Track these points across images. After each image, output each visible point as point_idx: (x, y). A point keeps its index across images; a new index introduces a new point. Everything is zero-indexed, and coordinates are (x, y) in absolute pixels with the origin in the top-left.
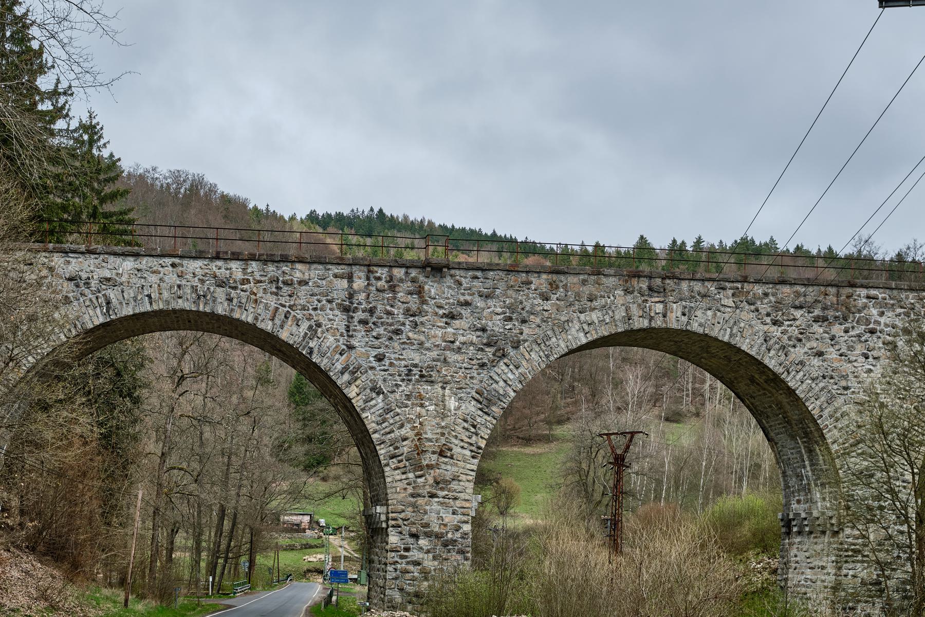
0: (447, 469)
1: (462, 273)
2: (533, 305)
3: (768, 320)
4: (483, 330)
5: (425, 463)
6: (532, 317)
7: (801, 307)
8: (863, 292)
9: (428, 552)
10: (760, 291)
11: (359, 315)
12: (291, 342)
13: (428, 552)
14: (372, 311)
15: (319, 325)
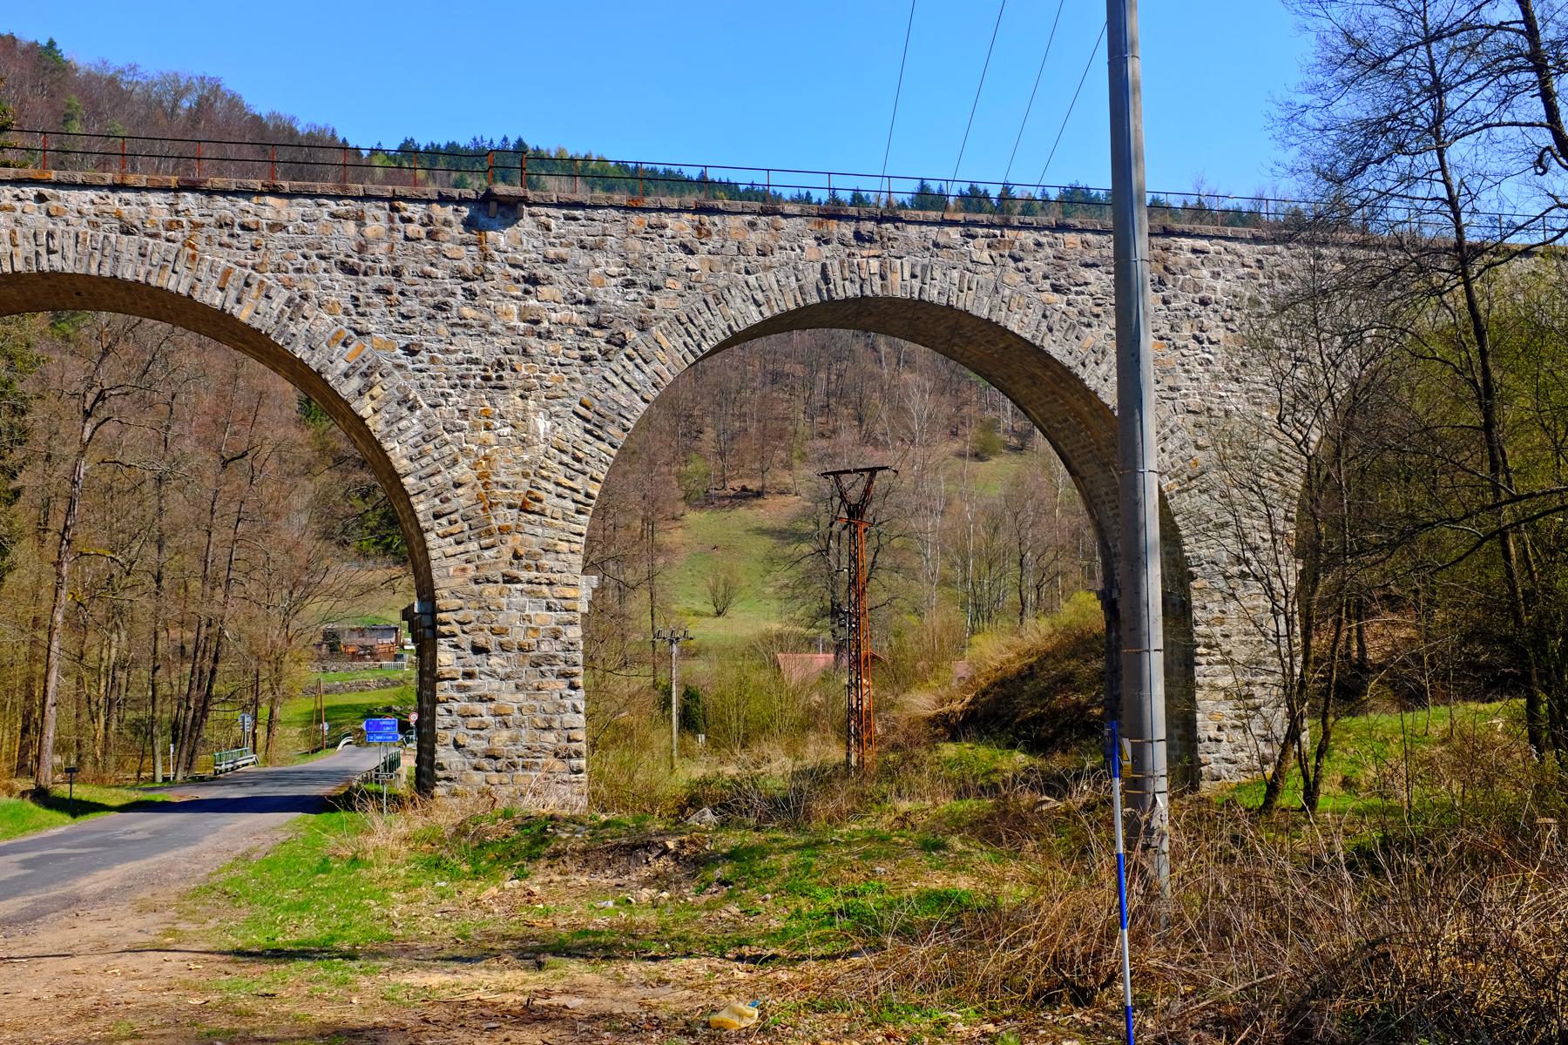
1: (552, 211)
2: (669, 263)
3: (1046, 285)
4: (589, 302)
5: (495, 524)
6: (670, 280)
7: (1094, 265)
8: (1187, 243)
9: (508, 677)
10: (1030, 242)
12: (256, 325)
13: (508, 677)
14: (397, 273)
15: (305, 297)
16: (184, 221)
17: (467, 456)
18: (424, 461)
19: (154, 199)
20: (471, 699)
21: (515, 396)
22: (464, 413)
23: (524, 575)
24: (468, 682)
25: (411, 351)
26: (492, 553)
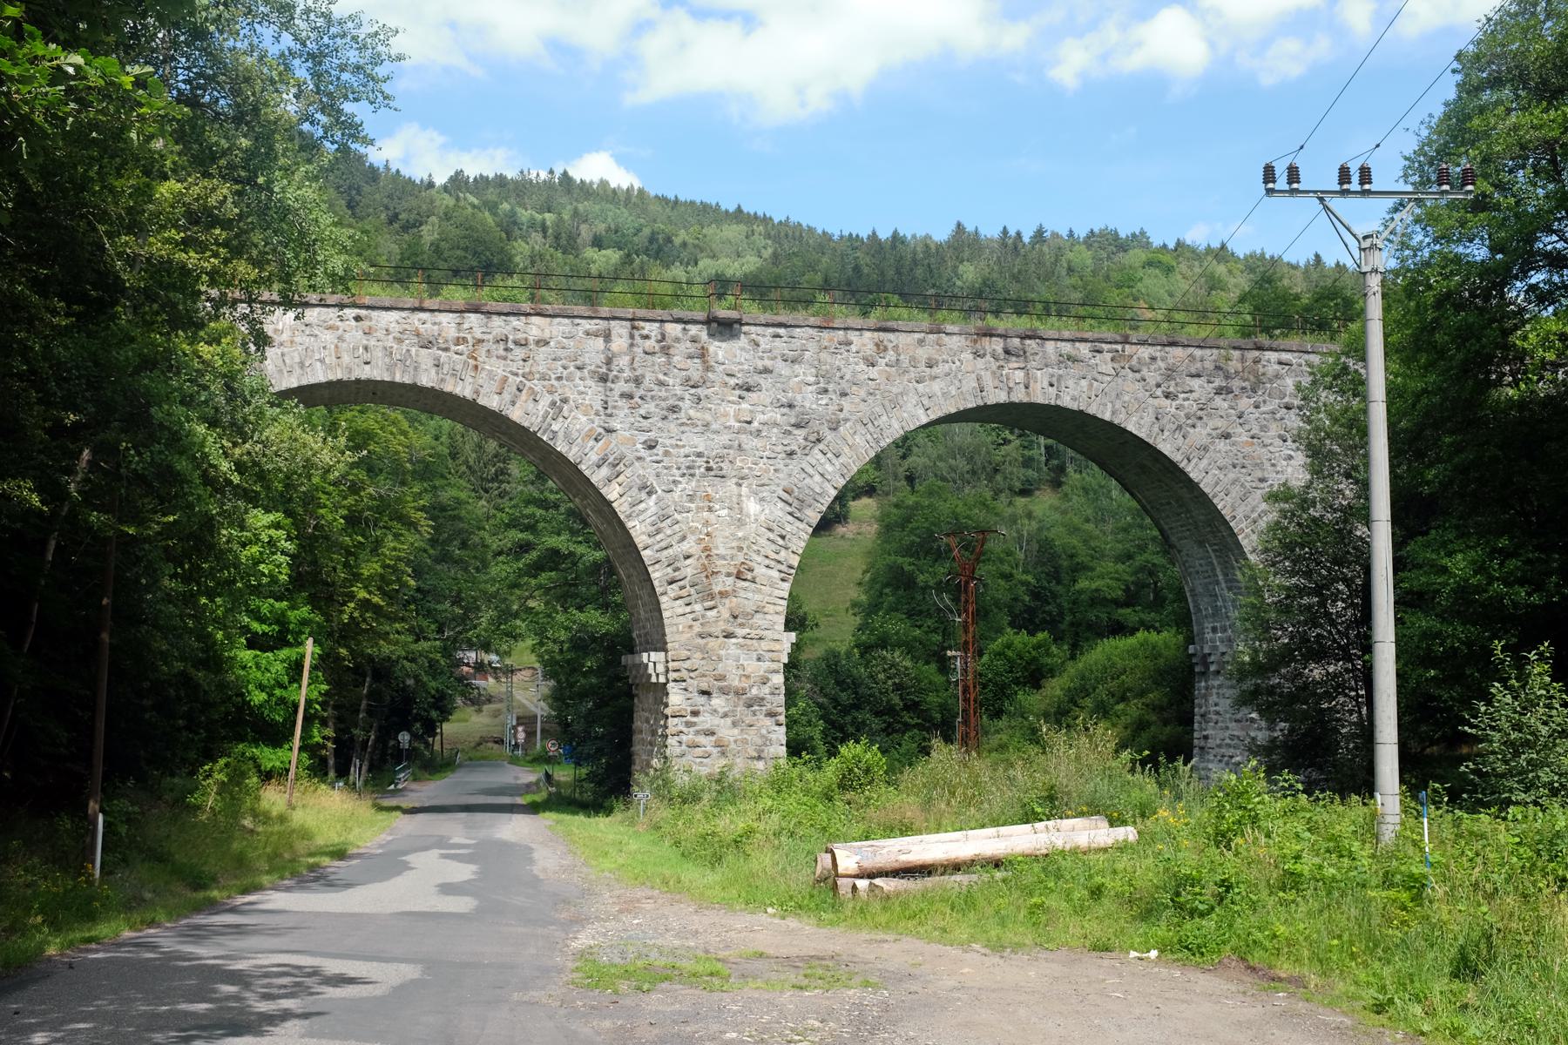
0: (748, 597)
1: (759, 329)
2: (854, 373)
3: (1159, 392)
4: (791, 406)
5: (716, 589)
7: (1199, 376)
8: (1273, 356)
9: (725, 715)
10: (1146, 356)
11: (622, 386)
12: (526, 424)
13: (725, 715)
14: (638, 381)
16: (469, 337)
17: (693, 533)
18: (658, 537)
19: (445, 318)
20: (697, 733)
21: (731, 483)
22: (691, 498)
23: (740, 632)
24: (694, 719)
25: (651, 446)
26: (713, 613)
